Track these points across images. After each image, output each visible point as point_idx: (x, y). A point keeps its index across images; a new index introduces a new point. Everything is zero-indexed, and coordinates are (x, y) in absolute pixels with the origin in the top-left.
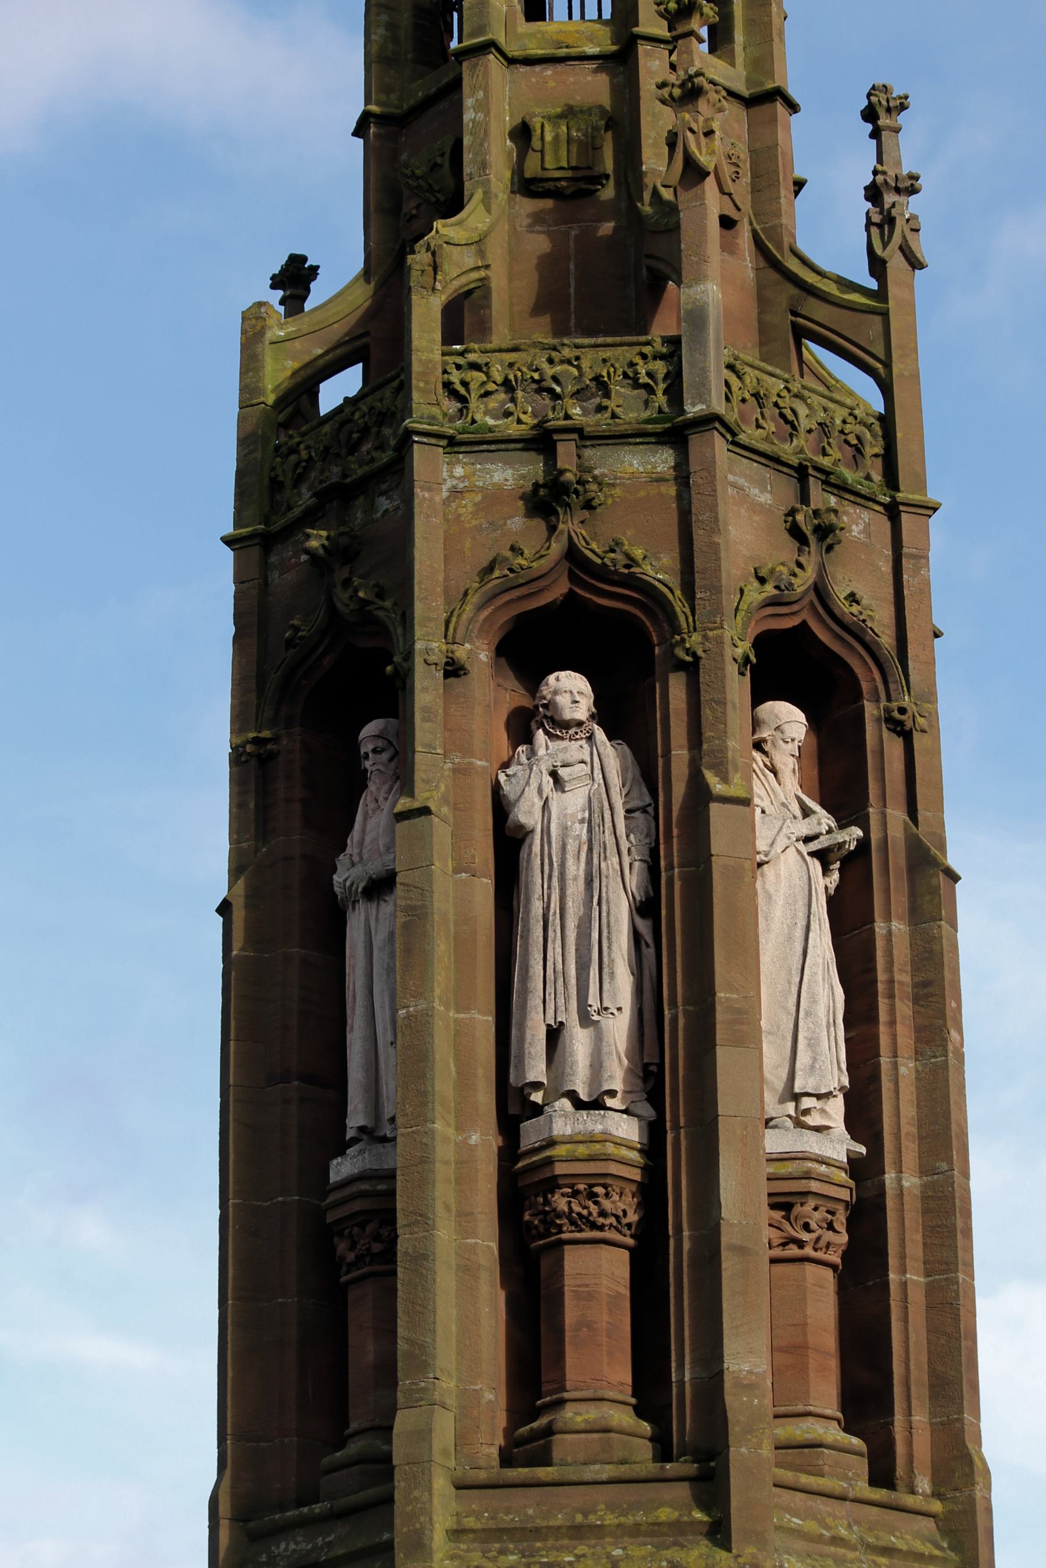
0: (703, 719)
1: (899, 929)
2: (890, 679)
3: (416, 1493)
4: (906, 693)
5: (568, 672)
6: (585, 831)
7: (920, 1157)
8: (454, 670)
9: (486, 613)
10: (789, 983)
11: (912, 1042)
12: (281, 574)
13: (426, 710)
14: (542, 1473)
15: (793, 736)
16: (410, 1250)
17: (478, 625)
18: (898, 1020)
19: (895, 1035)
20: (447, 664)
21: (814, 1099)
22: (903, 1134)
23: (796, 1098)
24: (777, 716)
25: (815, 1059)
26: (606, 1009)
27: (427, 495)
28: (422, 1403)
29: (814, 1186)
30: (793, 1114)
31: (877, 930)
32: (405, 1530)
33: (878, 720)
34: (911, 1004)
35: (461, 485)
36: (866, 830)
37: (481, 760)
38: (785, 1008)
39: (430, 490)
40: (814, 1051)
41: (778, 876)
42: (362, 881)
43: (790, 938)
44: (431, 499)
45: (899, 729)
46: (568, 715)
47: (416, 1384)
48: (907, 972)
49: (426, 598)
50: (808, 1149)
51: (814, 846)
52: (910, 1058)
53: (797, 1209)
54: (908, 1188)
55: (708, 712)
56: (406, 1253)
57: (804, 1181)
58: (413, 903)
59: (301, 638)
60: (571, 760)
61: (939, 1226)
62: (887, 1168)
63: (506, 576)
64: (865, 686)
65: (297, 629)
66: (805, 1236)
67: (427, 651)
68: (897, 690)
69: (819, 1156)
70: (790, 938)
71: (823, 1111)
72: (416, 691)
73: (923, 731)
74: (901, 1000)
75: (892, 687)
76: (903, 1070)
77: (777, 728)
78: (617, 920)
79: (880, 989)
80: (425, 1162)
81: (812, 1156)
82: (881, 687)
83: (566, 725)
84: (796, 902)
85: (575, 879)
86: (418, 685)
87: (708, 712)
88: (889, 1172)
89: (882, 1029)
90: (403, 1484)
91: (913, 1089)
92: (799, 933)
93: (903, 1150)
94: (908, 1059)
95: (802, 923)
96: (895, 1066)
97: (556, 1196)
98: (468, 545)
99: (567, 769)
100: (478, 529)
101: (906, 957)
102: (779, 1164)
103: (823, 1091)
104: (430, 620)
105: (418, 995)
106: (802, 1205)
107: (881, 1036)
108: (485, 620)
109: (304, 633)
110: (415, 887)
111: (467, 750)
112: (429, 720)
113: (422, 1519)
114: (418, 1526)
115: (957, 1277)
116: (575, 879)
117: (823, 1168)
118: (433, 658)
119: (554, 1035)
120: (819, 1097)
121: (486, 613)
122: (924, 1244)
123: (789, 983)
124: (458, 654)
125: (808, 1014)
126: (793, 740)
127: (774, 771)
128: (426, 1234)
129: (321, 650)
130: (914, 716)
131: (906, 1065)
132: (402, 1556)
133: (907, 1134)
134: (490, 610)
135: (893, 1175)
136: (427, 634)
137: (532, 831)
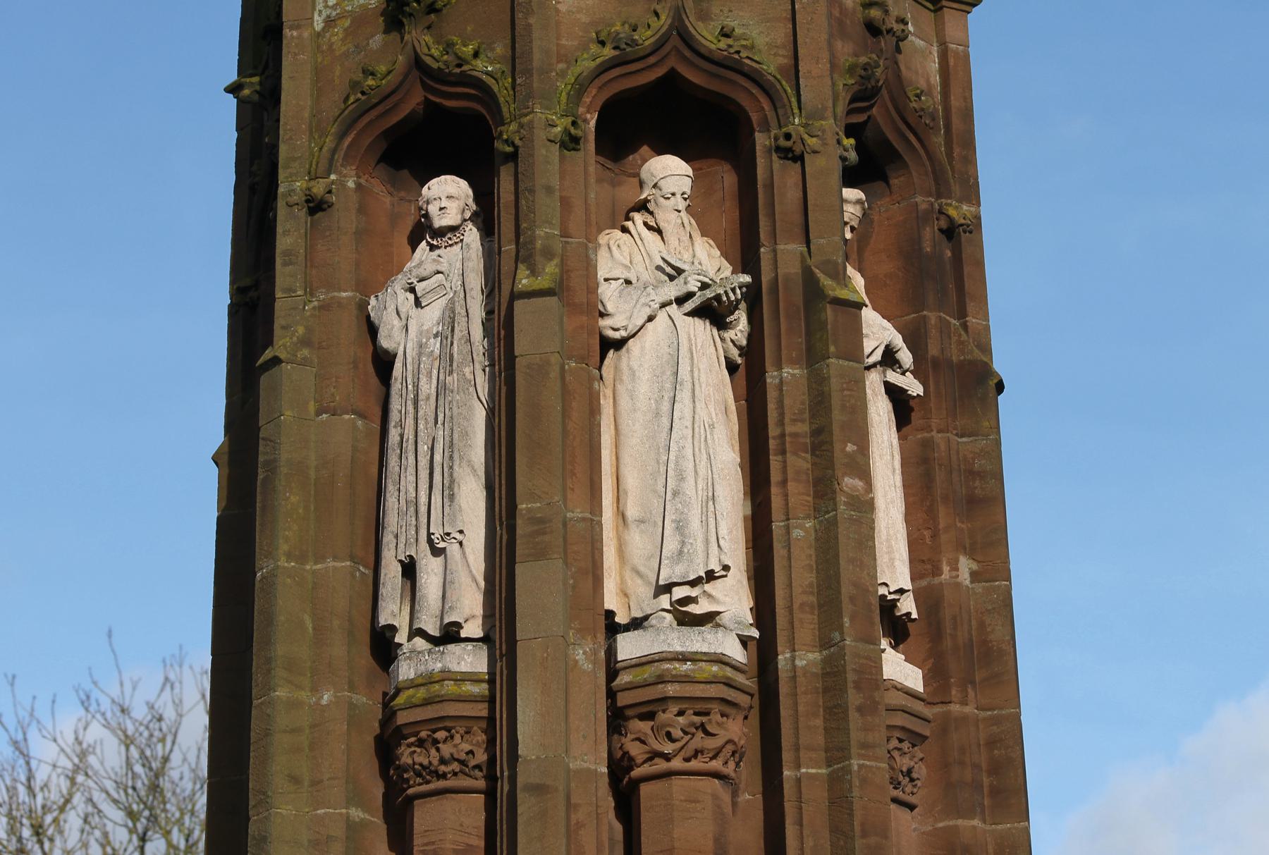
1: (793, 375)
2: (778, 105)
4: (796, 111)
5: (443, 177)
6: (438, 345)
7: (820, 629)
8: (316, 206)
9: (348, 140)
10: (658, 463)
11: (810, 499)
13: (287, 253)
15: (672, 190)
17: (342, 153)
18: (789, 477)
19: (786, 495)
20: (307, 201)
21: (687, 588)
22: (796, 606)
23: (668, 588)
24: (652, 175)
25: (683, 543)
26: (448, 534)
27: (295, 33)
29: (671, 690)
30: (669, 607)
31: (768, 380)
33: (769, 151)
34: (808, 456)
35: (334, 13)
36: (756, 276)
37: (345, 291)
38: (655, 491)
39: (298, 27)
40: (682, 535)
41: (643, 348)
43: (657, 414)
44: (300, 37)
45: (790, 155)
46: (439, 222)
48: (803, 421)
49: (291, 138)
50: (665, 648)
51: (689, 306)
52: (808, 517)
53: (662, 717)
54: (803, 668)
57: (660, 686)
60: (425, 274)
61: (835, 707)
62: (779, 649)
63: (358, 100)
64: (755, 117)
67: (291, 192)
68: (786, 113)
69: (682, 653)
70: (657, 414)
71: (709, 596)
72: (278, 237)
73: (815, 152)
74: (795, 454)
75: (780, 112)
76: (797, 533)
77: (655, 186)
78: (465, 434)
79: (771, 447)
81: (670, 656)
82: (770, 114)
83: (441, 233)
84: (663, 373)
85: (428, 398)
86: (279, 230)
88: (783, 653)
89: (774, 490)
91: (812, 552)
92: (666, 406)
93: (796, 624)
94: (804, 518)
95: (668, 396)
96: (788, 530)
98: (337, 73)
99: (424, 283)
100: (346, 55)
101: (803, 403)
102: (638, 669)
103: (692, 577)
104: (294, 159)
106: (664, 711)
107: (773, 498)
108: (349, 146)
111: (331, 286)
112: (291, 263)
115: (850, 765)
116: (428, 398)
117: (688, 666)
118: (295, 198)
120: (693, 583)
121: (348, 140)
122: (825, 729)
123: (658, 463)
124: (315, 190)
125: (675, 494)
126: (673, 194)
127: (659, 231)
130: (802, 139)
131: (801, 527)
133: (802, 605)
134: (352, 136)
135: (788, 655)
136: (291, 175)
137: (395, 356)
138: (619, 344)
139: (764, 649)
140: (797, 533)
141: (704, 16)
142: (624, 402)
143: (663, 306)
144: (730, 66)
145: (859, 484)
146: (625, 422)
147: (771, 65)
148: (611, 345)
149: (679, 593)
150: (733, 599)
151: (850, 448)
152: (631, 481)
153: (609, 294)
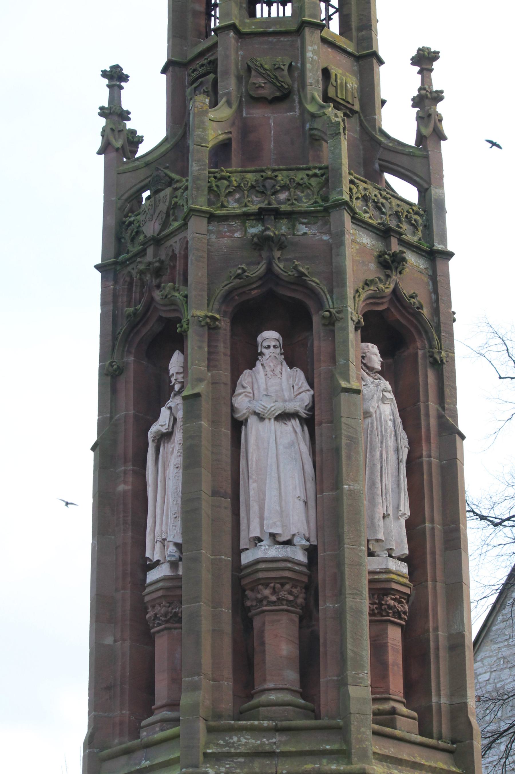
0: (445, 393)
3: (363, 729)
12: (216, 238)
14: (388, 730)
16: (353, 607)
28: (362, 685)
32: (357, 746)
42: (280, 410)
47: (358, 674)
55: (448, 390)
56: (351, 608)
58: (351, 435)
59: (247, 276)
65: (244, 271)
80: (360, 565)
87: (448, 390)
90: (356, 723)
97: (389, 598)
105: (356, 481)
109: (249, 274)
110: (352, 428)
113: (367, 743)
114: (365, 746)
128: (360, 600)
129: (254, 286)
132: (356, 759)
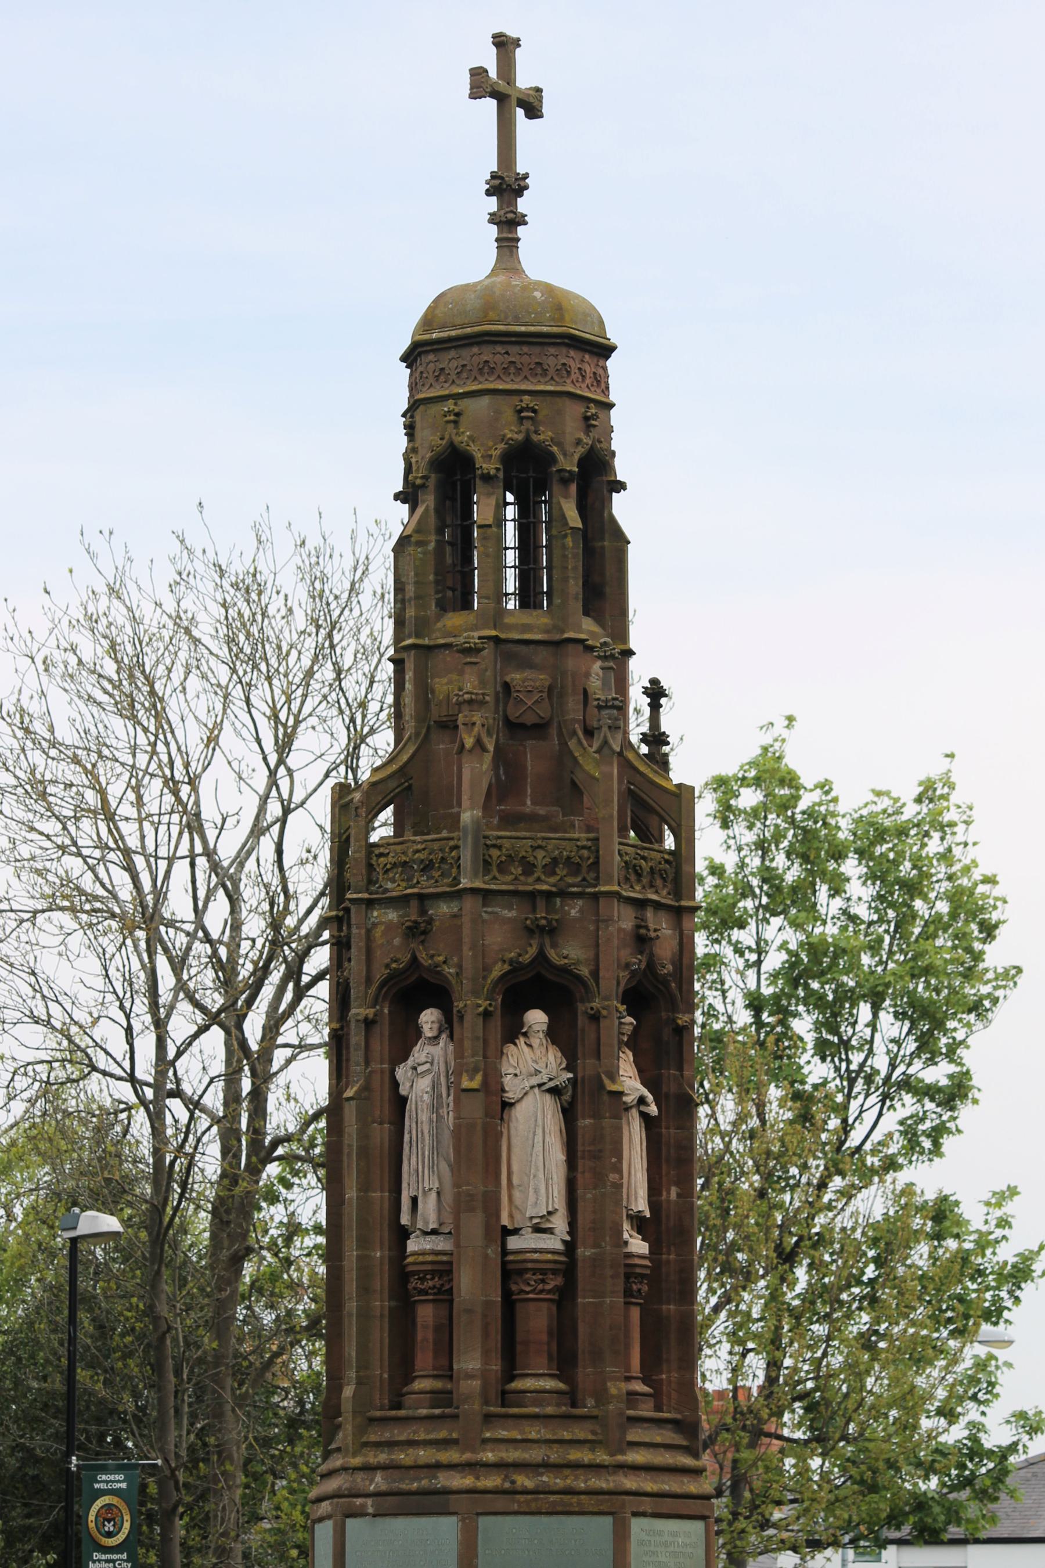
66: (528, 1289)
92: (531, 1135)
119: (414, 1200)
138: (512, 1105)
139: (570, 1247)
140: (586, 1195)
141: (554, 945)
142: (513, 1132)
143: (532, 1087)
144: (565, 970)
145: (617, 1176)
146: (514, 1141)
147: (585, 971)
148: (507, 1105)
149: (535, 1221)
150: (560, 1224)
151: (614, 1160)
152: (515, 1167)
153: (507, 1080)
